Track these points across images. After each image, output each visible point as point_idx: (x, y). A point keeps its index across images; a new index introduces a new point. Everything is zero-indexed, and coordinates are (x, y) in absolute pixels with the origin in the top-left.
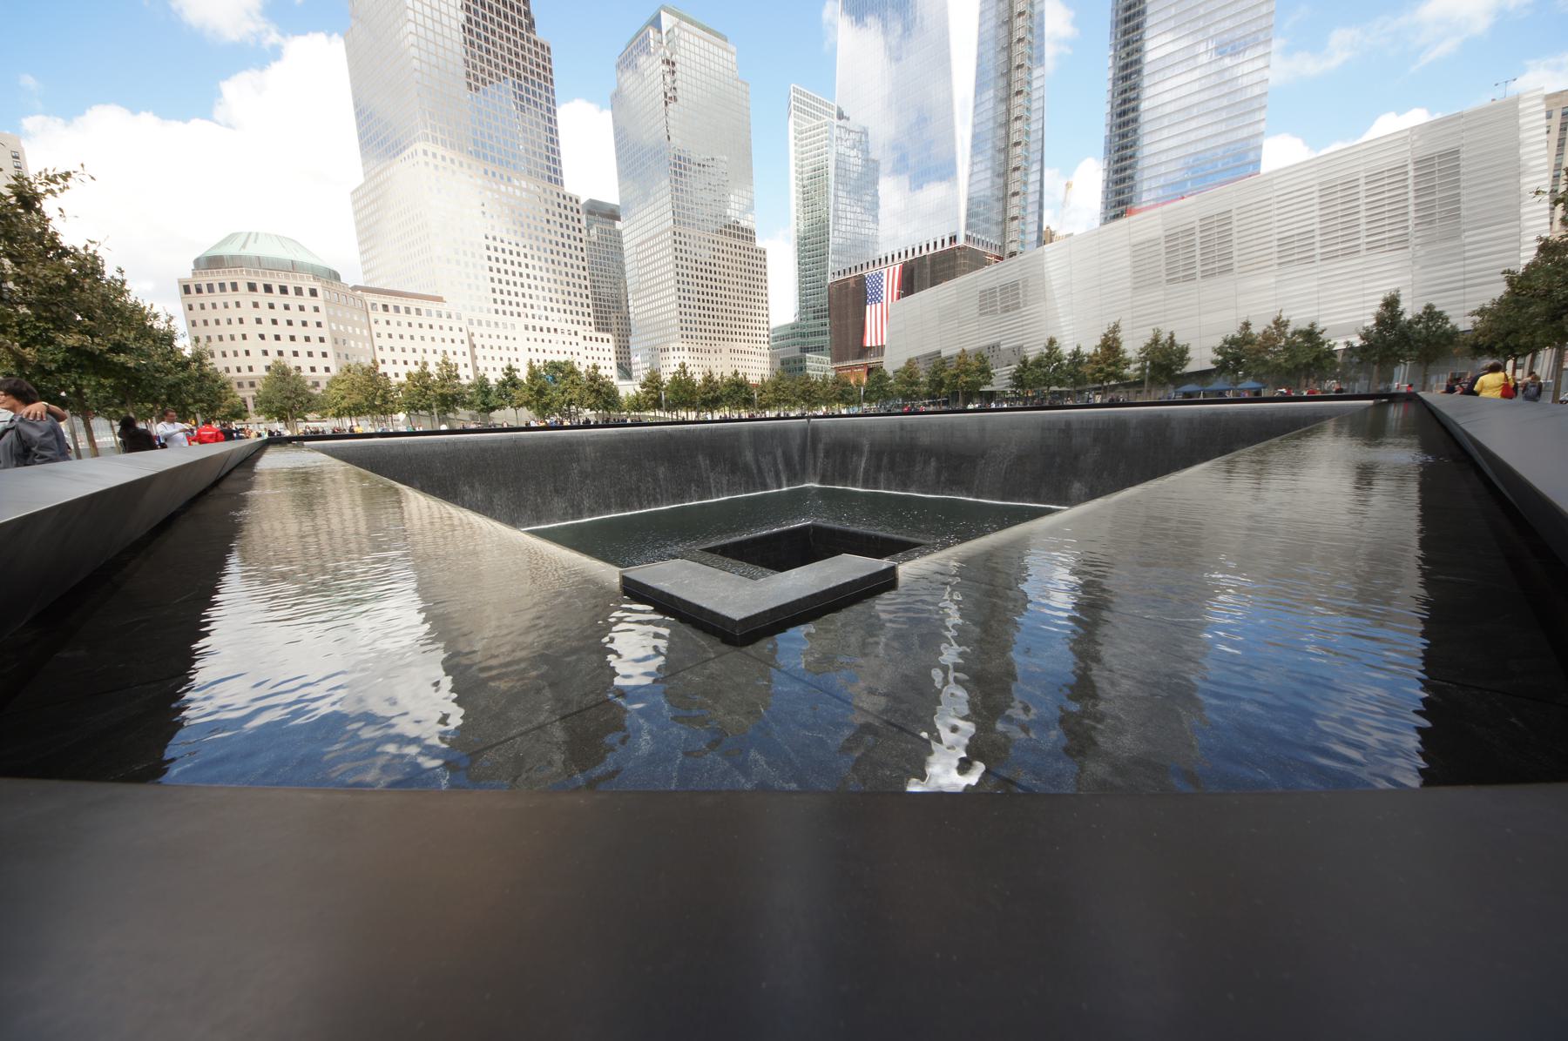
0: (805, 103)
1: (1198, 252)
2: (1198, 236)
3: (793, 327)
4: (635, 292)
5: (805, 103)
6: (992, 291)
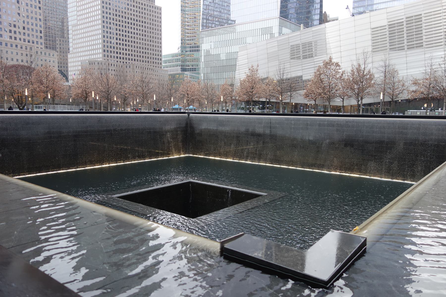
3: (176, 55)
4: (74, 26)
6: (298, 46)
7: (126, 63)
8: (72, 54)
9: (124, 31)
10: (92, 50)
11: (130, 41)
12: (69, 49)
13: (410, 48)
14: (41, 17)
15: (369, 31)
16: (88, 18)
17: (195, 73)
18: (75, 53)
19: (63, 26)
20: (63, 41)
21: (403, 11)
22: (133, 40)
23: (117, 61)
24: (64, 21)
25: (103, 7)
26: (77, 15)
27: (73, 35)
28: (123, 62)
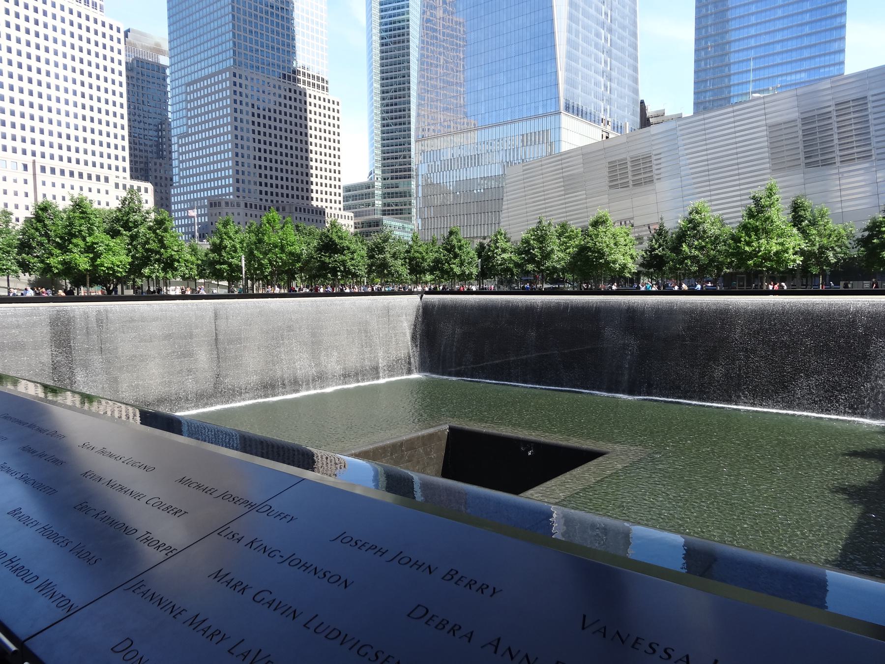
4: (181, 136)
7: (277, 201)
8: (177, 187)
9: (273, 145)
10: (214, 180)
11: (284, 163)
12: (172, 179)
16: (208, 121)
18: (183, 186)
20: (161, 165)
21: (829, 92)
22: (289, 159)
23: (261, 200)
25: (235, 92)
26: (186, 116)
27: (180, 154)
28: (272, 201)
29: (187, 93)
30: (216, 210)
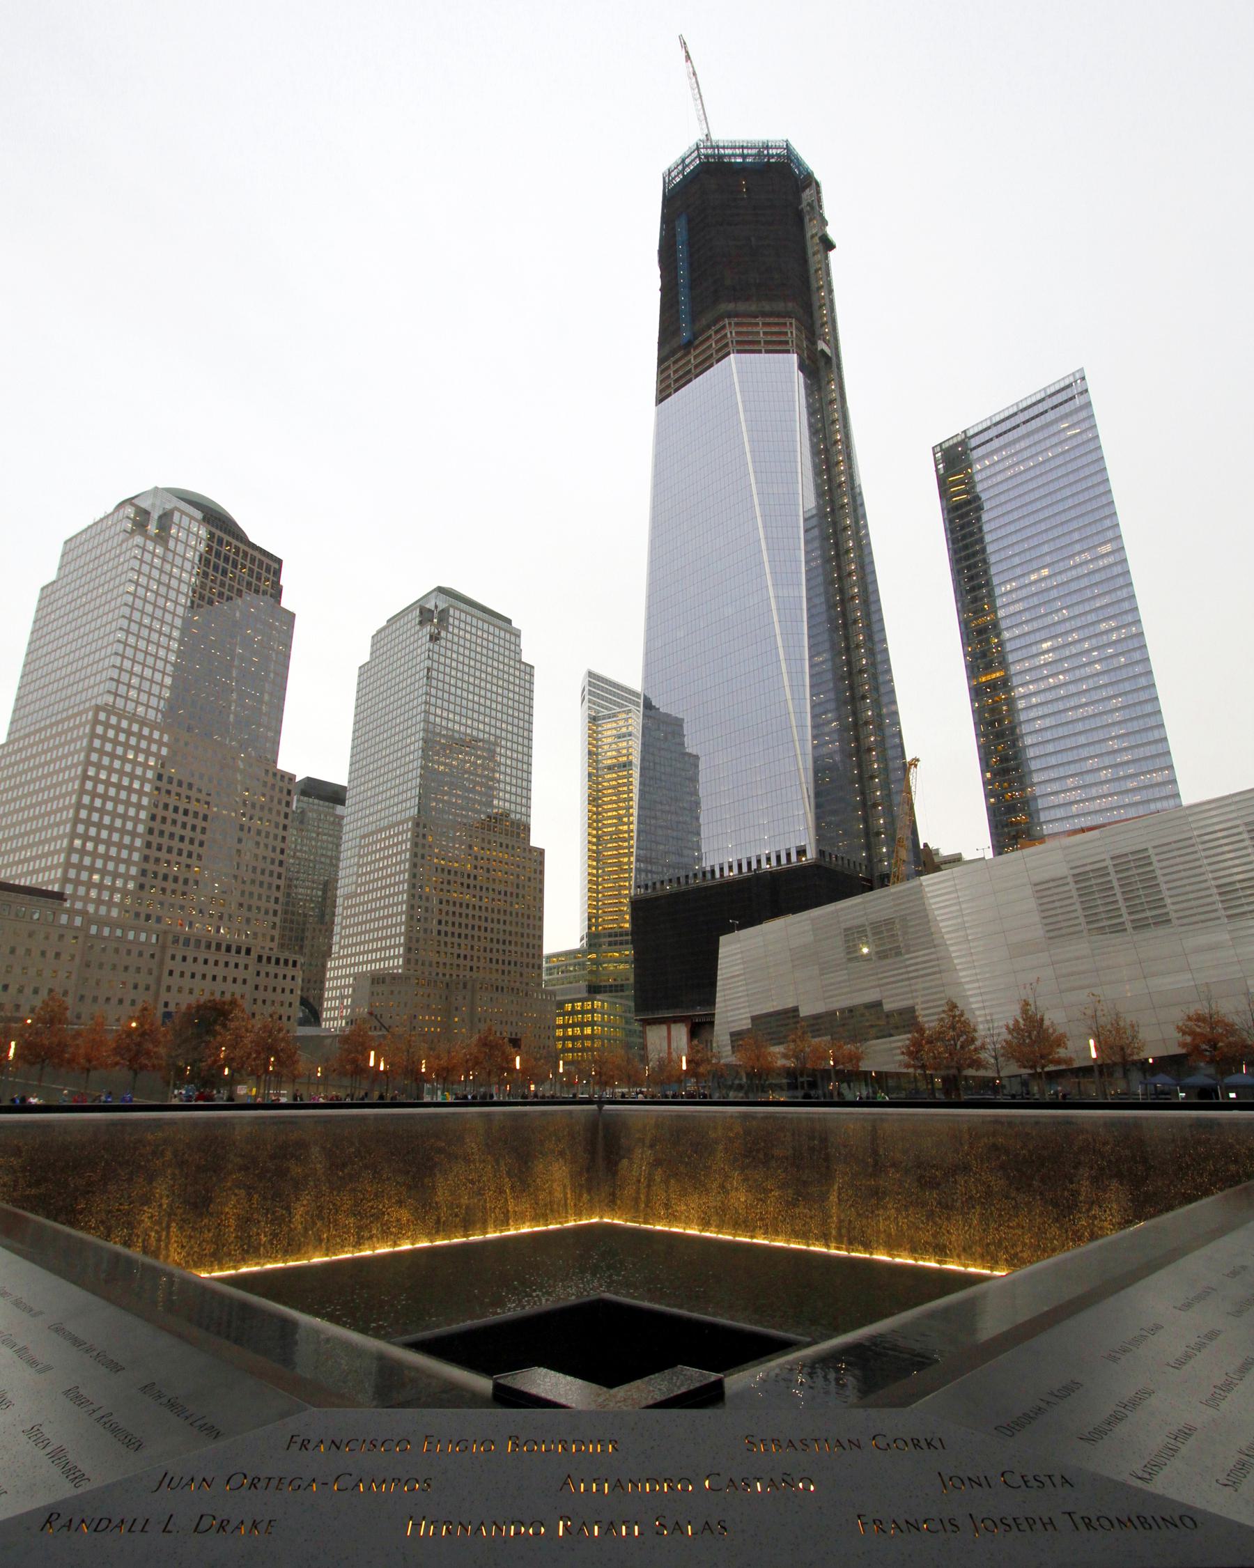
0: (602, 689)
1: (1119, 897)
2: (1113, 877)
4: (347, 897)
5: (602, 689)
8: (335, 959)
13: (1140, 926)
14: (282, 883)
15: (1028, 891)
17: (621, 997)
19: (324, 899)
24: (329, 887)
29: (361, 847)
30: (380, 988)
